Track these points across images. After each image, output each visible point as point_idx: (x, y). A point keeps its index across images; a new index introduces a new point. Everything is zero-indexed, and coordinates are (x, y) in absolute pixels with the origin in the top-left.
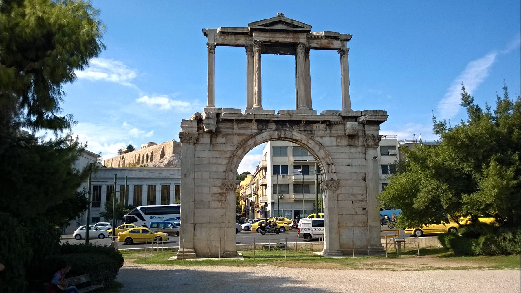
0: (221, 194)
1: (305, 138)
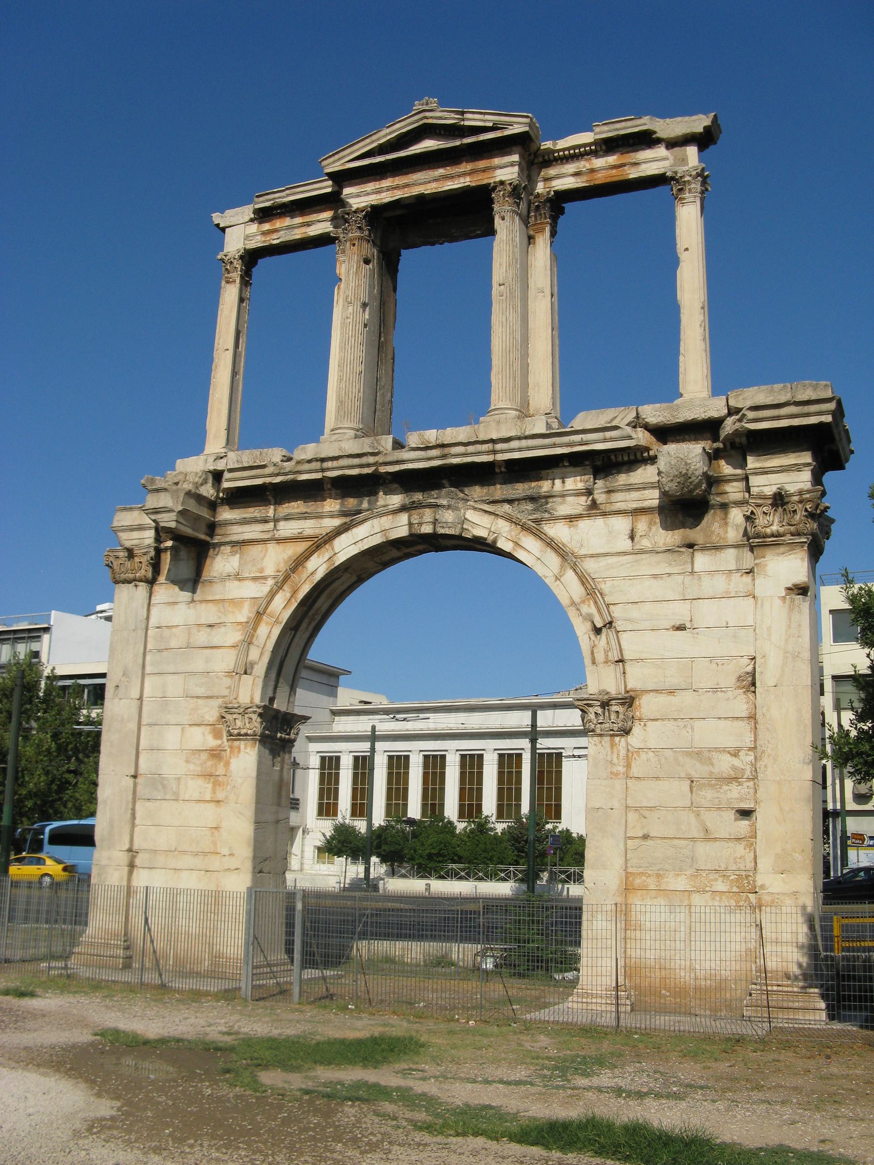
0: (215, 754)
1: (507, 529)
